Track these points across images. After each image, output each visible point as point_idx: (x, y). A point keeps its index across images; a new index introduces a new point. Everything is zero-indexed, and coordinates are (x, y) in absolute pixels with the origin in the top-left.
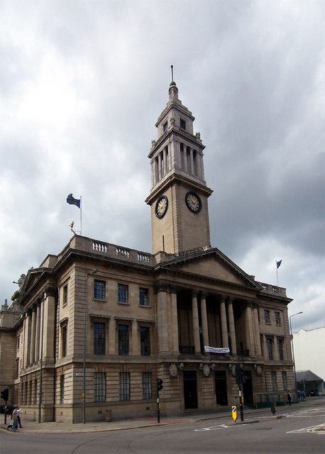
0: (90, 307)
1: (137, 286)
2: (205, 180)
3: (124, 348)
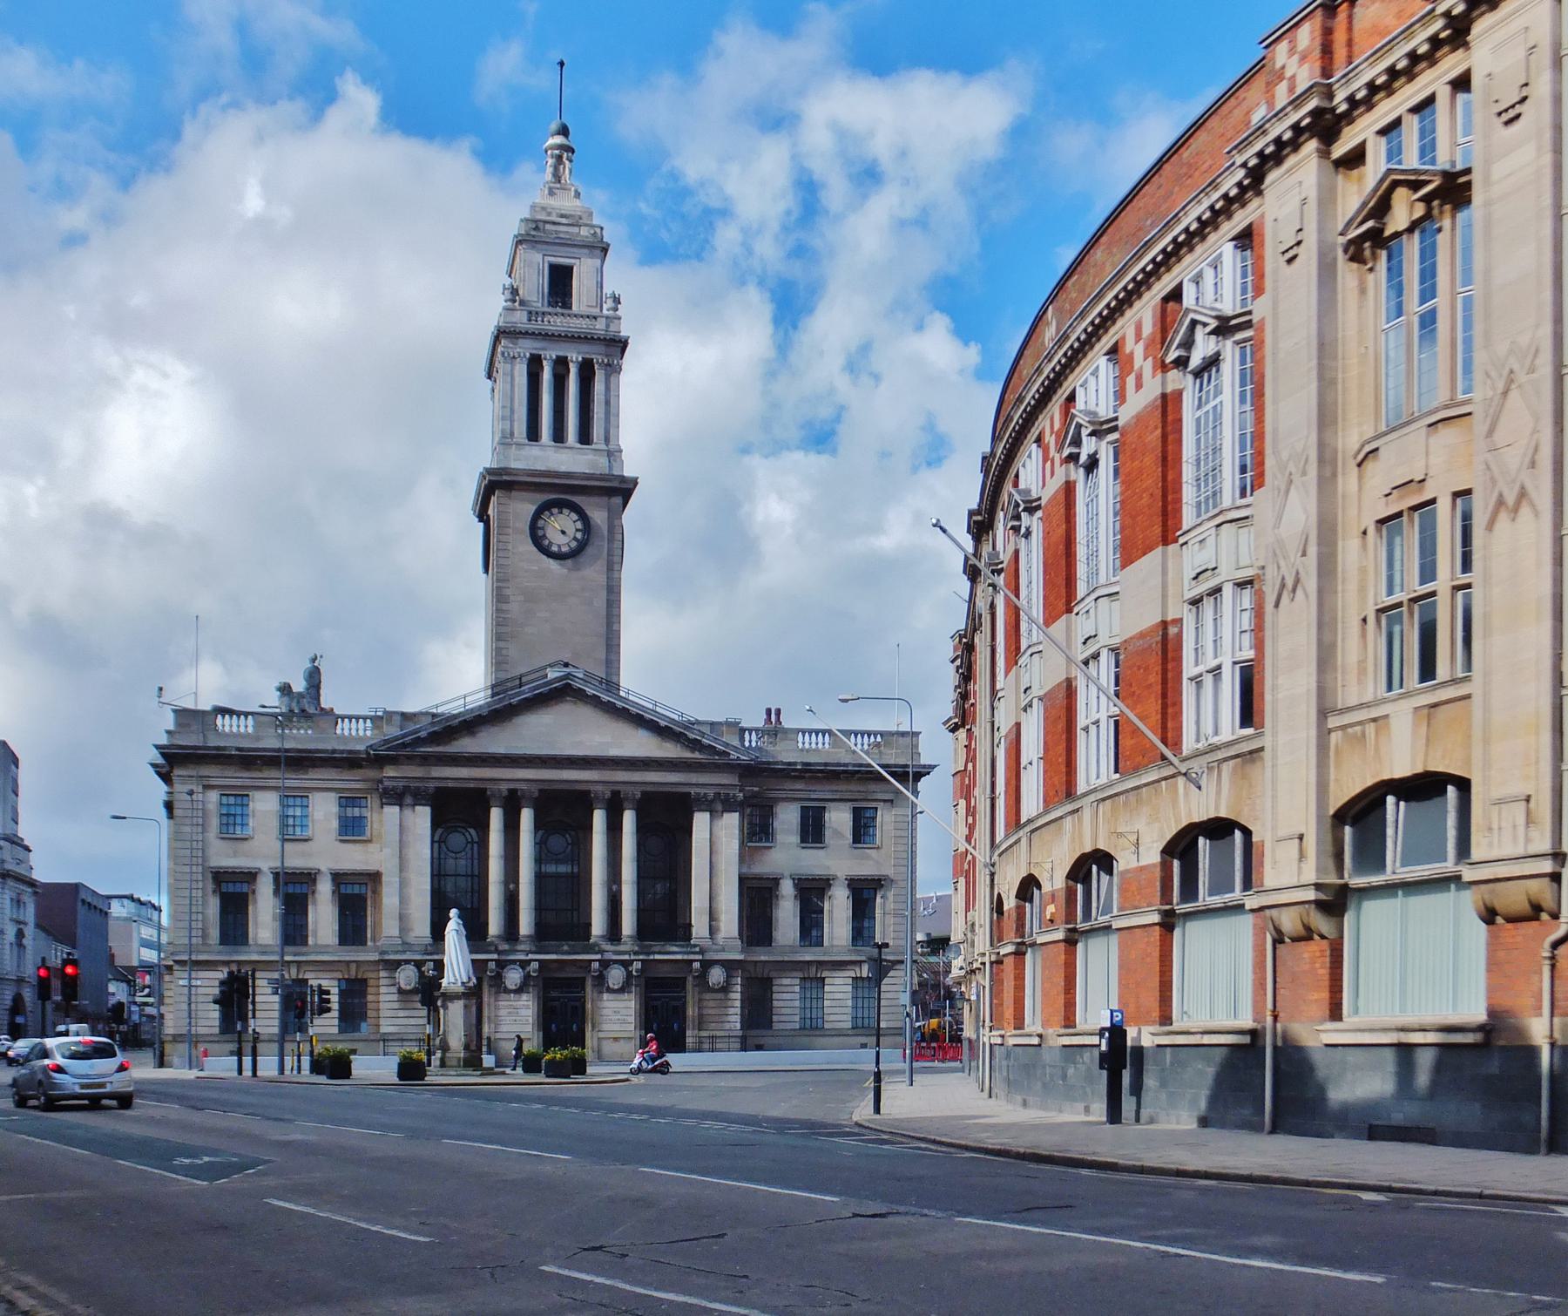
1: (333, 796)
3: (294, 928)
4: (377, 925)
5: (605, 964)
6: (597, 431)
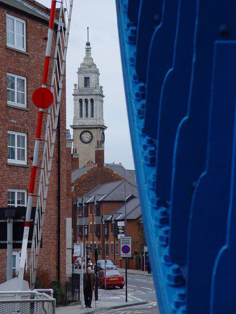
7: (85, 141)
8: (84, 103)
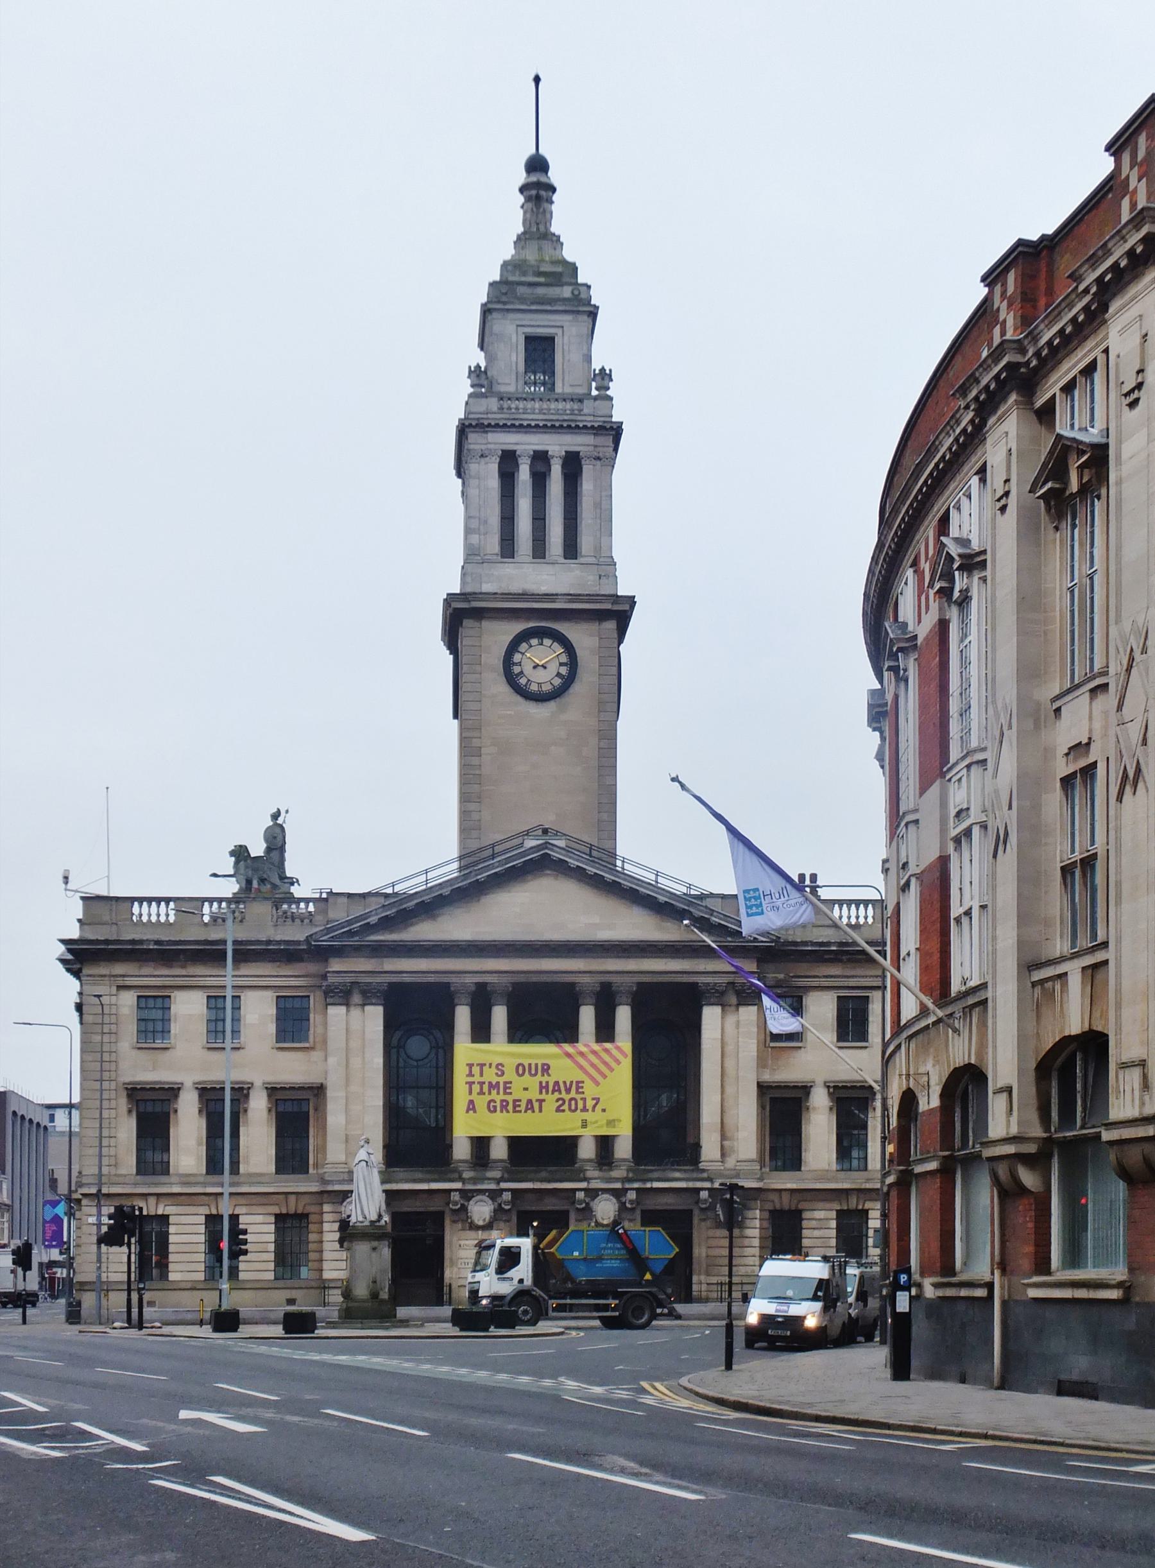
0: (124, 1065)
2: (619, 552)
4: (322, 1149)
5: (593, 1193)
6: (586, 542)
7: (534, 688)
8: (524, 474)
